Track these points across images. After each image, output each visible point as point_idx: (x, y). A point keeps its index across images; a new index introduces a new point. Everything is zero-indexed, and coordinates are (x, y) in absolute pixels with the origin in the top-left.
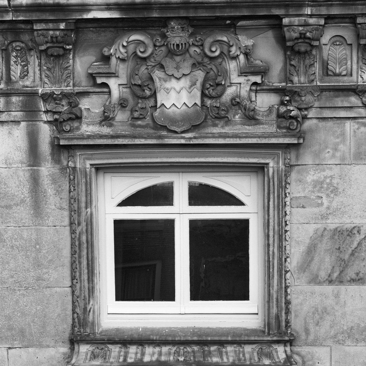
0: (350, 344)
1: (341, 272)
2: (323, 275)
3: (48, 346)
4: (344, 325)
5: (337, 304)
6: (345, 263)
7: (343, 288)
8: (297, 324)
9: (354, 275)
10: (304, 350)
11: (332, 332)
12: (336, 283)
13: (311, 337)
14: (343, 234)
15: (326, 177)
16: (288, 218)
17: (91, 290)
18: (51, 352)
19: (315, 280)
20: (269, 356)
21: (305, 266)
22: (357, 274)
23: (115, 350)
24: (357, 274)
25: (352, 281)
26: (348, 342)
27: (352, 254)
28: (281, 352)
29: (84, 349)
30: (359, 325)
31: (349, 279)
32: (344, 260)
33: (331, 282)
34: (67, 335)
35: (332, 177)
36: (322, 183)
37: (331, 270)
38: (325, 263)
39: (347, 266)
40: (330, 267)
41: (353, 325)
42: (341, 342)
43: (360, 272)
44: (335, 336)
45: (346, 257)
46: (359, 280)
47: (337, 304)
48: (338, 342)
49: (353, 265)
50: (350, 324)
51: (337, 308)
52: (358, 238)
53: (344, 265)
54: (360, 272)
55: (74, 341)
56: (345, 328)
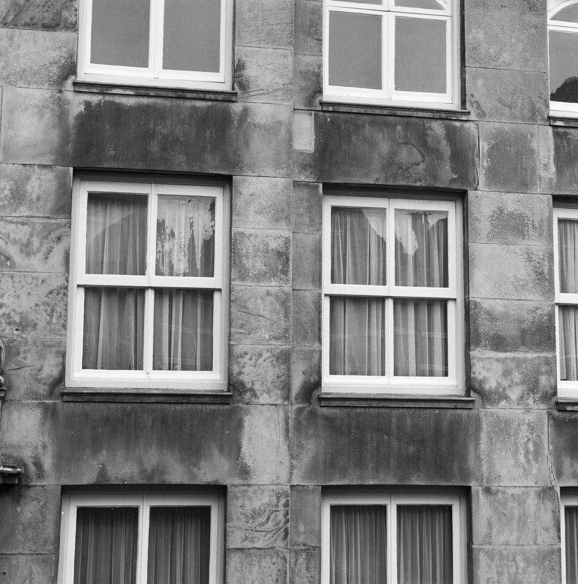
0: (21, 86)
1: (16, 16)
4: (16, 67)
5: (10, 46)
6: (20, 8)
7: (17, 31)
9: (28, 20)
11: (5, 74)
12: (11, 26)
22: (32, 19)
24: (32, 19)
25: (26, 26)
26: (21, 84)
30: (31, 68)
31: (23, 23)
32: (19, 4)
37: (6, 13)
39: (22, 10)
40: (5, 11)
41: (25, 67)
42: (14, 83)
43: (34, 17)
44: (8, 77)
46: (33, 25)
47: (10, 46)
48: (10, 83)
49: (28, 10)
50: (23, 67)
51: (10, 49)
54: (34, 17)
56: (18, 70)
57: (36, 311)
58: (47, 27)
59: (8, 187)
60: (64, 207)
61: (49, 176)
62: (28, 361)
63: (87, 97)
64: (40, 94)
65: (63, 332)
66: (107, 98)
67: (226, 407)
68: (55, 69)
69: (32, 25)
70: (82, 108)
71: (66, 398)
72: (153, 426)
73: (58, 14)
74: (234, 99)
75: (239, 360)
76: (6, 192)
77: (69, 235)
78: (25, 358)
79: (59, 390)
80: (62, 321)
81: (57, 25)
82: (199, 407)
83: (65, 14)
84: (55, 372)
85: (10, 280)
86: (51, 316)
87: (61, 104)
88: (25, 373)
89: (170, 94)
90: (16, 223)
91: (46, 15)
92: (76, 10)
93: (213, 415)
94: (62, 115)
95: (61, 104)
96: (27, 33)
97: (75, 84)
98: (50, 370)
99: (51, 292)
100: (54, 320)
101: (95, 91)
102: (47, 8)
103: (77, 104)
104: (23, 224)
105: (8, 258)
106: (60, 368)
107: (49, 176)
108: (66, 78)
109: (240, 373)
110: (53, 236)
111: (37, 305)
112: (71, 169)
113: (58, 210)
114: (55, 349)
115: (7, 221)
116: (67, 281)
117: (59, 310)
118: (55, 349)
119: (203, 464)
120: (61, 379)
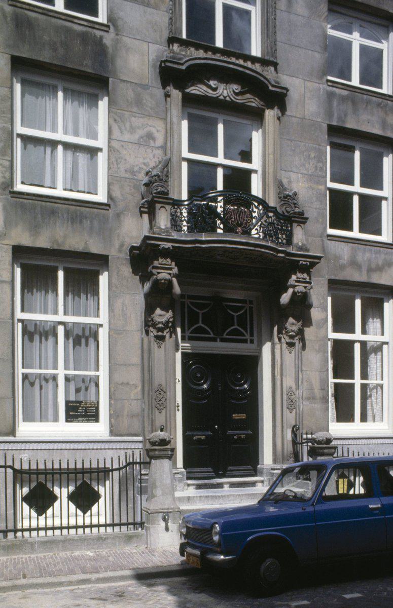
71: (329, 238)
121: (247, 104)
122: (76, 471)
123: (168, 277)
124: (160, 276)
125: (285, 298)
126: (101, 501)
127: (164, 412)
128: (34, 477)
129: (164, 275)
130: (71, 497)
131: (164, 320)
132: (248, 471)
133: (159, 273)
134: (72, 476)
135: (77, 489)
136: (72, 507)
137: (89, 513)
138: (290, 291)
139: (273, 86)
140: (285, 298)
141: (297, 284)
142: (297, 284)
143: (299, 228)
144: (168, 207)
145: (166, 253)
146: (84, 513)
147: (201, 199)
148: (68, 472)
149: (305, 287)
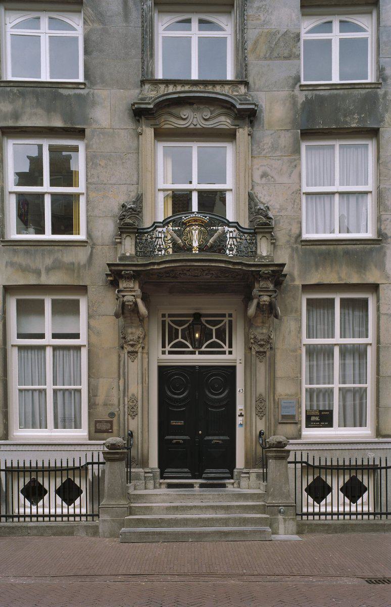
1: (271, 53)
2: (262, 55)
3: (130, 89)
8: (250, 80)
10: (252, 93)
13: (257, 86)
14: (272, 34)
15: (263, 5)
16: (246, 21)
17: (152, 56)
18: (132, 92)
19: (258, 58)
20: (238, 92)
21: (254, 49)
23: (162, 87)
24: (278, 54)
27: (276, 44)
28: (242, 89)
29: (147, 86)
33: (265, 58)
34: (140, 78)
35: (266, 5)
36: (261, 8)
38: (263, 49)
45: (273, 46)
52: (279, 36)
53: (272, 50)
55: (143, 82)
57: (287, 202)
58: (285, 58)
59: (270, 142)
60: (297, 151)
61: (289, 134)
62: (284, 227)
63: (306, 92)
64: (284, 93)
65: (299, 212)
66: (318, 92)
67: (378, 246)
68: (291, 81)
69: (278, 57)
70: (304, 99)
71: (303, 243)
72: (343, 256)
73: (291, 50)
74: (380, 86)
75: (385, 222)
76: (270, 144)
77: (300, 164)
78: (283, 225)
79: (299, 240)
80: (299, 207)
81: (291, 56)
82: (366, 246)
83: (294, 50)
84: (297, 232)
85: (274, 188)
86: (294, 204)
87: (294, 98)
88: (283, 232)
89: (347, 87)
90: (275, 159)
91: (285, 51)
92: (299, 48)
93: (371, 250)
94: (294, 103)
95: (294, 98)
96: (278, 62)
97: (301, 86)
98: (295, 231)
99: (293, 193)
100: (295, 206)
101: (310, 89)
102: (285, 48)
103: (301, 97)
104: (278, 160)
105: (272, 177)
106: (299, 229)
107: (289, 134)
108: (296, 84)
109: (385, 229)
110: (294, 164)
111: (287, 199)
112: (299, 131)
113: (294, 152)
114: (296, 221)
115: (270, 159)
116: (300, 186)
117: (297, 201)
118: (296, 221)
119: (367, 273)
120: (300, 235)
121: (216, 127)
122: (61, 469)
123: (131, 298)
124: (125, 299)
125: (252, 310)
126: (83, 495)
127: (136, 418)
128: (27, 474)
129: (129, 298)
130: (58, 492)
131: (135, 337)
132: (212, 475)
133: (124, 296)
134: (59, 473)
135: (63, 484)
136: (59, 499)
137: (73, 505)
138: (255, 302)
139: (240, 104)
140: (252, 310)
141: (262, 293)
142: (262, 293)
143: (264, 240)
144: (133, 236)
145: (129, 278)
146: (69, 504)
147: (162, 225)
148: (56, 470)
149: (270, 296)
